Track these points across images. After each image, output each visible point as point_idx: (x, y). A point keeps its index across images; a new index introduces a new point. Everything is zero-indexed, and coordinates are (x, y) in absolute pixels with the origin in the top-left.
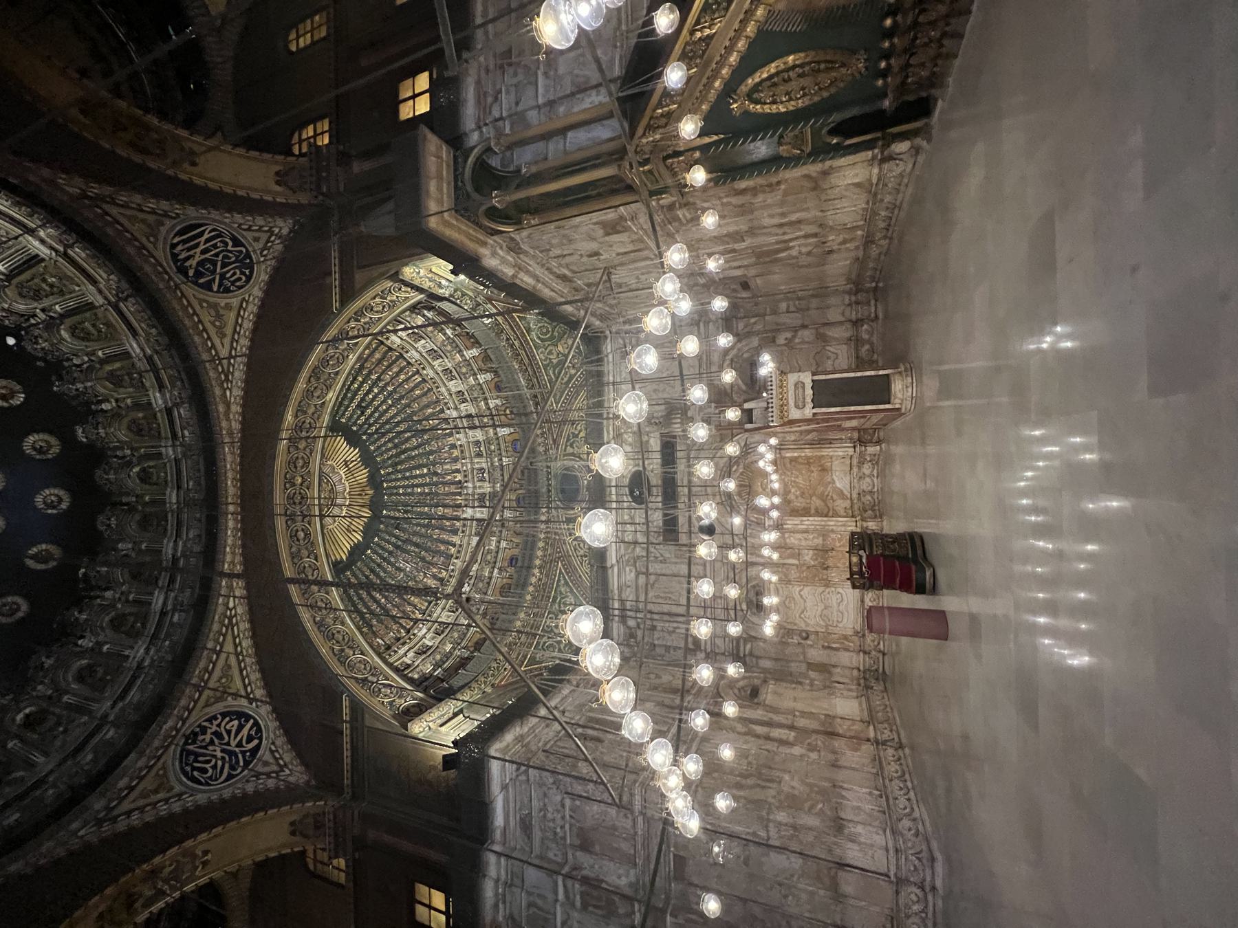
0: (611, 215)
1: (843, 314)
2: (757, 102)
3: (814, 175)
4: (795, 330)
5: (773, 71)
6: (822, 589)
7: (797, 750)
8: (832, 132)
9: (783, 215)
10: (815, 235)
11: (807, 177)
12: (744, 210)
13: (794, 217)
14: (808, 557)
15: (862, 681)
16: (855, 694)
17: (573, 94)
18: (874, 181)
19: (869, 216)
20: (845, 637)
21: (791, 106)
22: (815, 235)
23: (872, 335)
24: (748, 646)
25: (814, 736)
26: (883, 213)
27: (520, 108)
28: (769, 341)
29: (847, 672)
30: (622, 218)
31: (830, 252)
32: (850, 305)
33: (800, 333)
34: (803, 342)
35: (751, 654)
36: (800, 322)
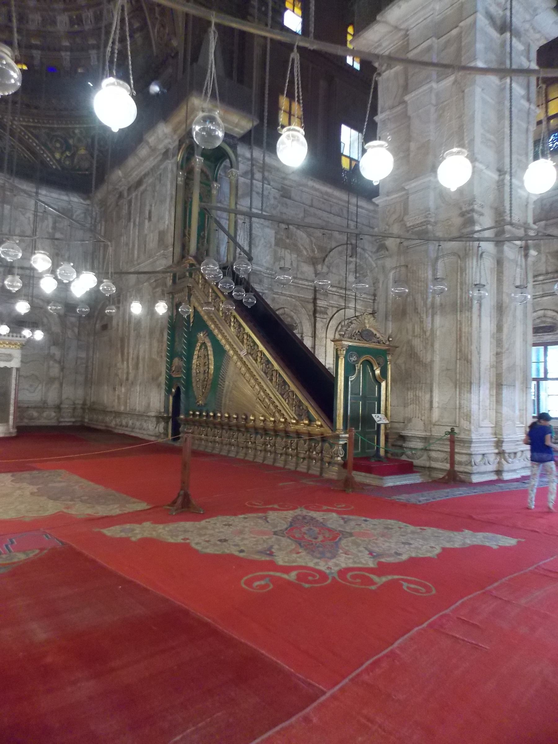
0: (170, 240)
2: (201, 347)
3: (160, 379)
4: (61, 363)
5: (210, 357)
8: (178, 390)
9: (144, 358)
10: (127, 379)
11: (160, 374)
12: (152, 333)
13: (141, 365)
17: (251, 234)
18: (149, 414)
19: (132, 414)
21: (194, 366)
22: (127, 379)
26: (130, 423)
27: (254, 193)
28: (53, 339)
30: (166, 247)
32: (74, 404)
33: (57, 365)
34: (49, 367)
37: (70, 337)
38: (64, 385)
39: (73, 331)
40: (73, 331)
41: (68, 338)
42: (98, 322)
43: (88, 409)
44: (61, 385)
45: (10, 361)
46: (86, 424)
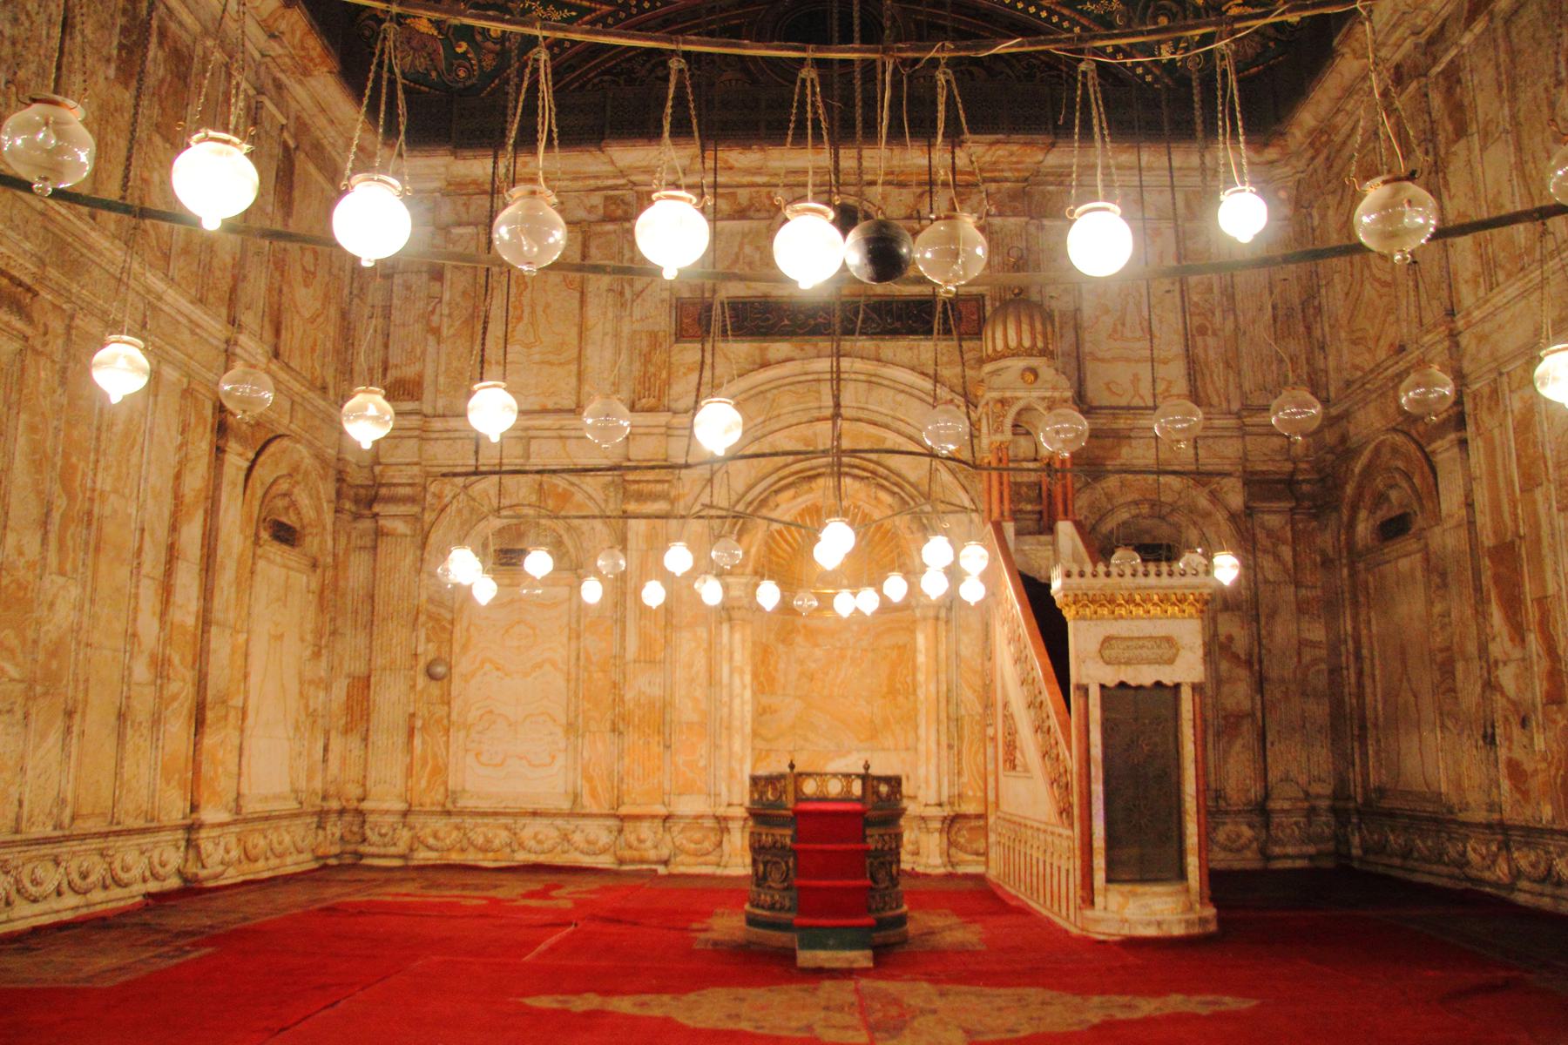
1: (1286, 779)
6: (563, 720)
7: (148, 627)
14: (643, 685)
15: (334, 805)
16: (302, 784)
20: (439, 771)
23: (1224, 848)
24: (401, 527)
25: (190, 675)
29: (354, 772)
31: (1490, 740)
32: (1307, 794)
33: (1243, 673)
35: (379, 533)
36: (1273, 673)
37: (1271, 578)
38: (1270, 738)
39: (1277, 557)
40: (1277, 557)
41: (1266, 581)
42: (1363, 514)
43: (1358, 811)
44: (1262, 736)
45: (1171, 661)
46: (1356, 865)
